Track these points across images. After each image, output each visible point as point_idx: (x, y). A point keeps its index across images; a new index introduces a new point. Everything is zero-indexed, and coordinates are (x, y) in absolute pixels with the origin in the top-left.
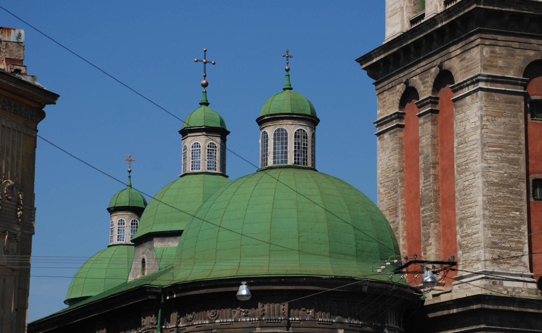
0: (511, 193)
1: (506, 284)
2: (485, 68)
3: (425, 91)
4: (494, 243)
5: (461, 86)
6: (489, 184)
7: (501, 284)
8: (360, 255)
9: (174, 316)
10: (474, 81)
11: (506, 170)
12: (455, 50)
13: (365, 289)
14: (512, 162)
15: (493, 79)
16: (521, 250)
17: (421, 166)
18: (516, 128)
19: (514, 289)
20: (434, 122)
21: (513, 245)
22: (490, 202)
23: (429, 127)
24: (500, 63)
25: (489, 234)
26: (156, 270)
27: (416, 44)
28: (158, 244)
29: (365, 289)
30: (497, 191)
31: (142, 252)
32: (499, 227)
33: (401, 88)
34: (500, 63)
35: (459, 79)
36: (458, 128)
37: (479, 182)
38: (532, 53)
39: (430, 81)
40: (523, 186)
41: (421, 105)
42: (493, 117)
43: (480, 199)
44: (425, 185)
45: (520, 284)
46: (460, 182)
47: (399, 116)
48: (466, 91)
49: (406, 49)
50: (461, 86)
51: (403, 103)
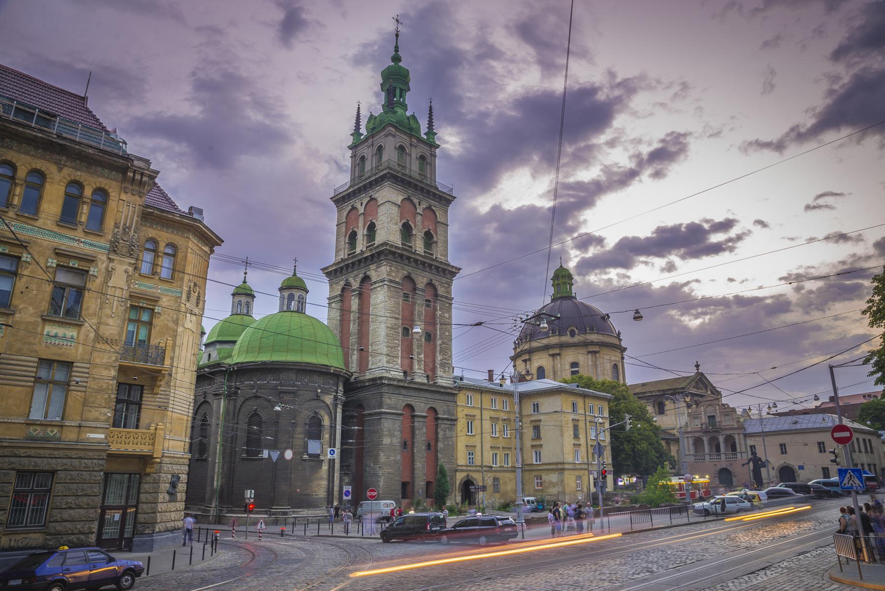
2: (388, 275)
3: (355, 284)
5: (375, 283)
6: (388, 327)
9: (234, 379)
10: (383, 281)
11: (393, 321)
12: (373, 267)
14: (396, 318)
15: (391, 281)
17: (352, 318)
18: (398, 304)
20: (360, 299)
22: (387, 335)
23: (357, 300)
25: (386, 349)
26: (218, 359)
27: (353, 264)
28: (218, 346)
31: (210, 349)
33: (342, 283)
35: (374, 280)
36: (372, 301)
37: (383, 326)
39: (359, 280)
40: (400, 330)
41: (354, 291)
42: (390, 297)
43: (383, 333)
44: (353, 327)
46: (372, 327)
47: (341, 295)
48: (378, 285)
49: (347, 266)
50: (375, 283)
51: (343, 290)
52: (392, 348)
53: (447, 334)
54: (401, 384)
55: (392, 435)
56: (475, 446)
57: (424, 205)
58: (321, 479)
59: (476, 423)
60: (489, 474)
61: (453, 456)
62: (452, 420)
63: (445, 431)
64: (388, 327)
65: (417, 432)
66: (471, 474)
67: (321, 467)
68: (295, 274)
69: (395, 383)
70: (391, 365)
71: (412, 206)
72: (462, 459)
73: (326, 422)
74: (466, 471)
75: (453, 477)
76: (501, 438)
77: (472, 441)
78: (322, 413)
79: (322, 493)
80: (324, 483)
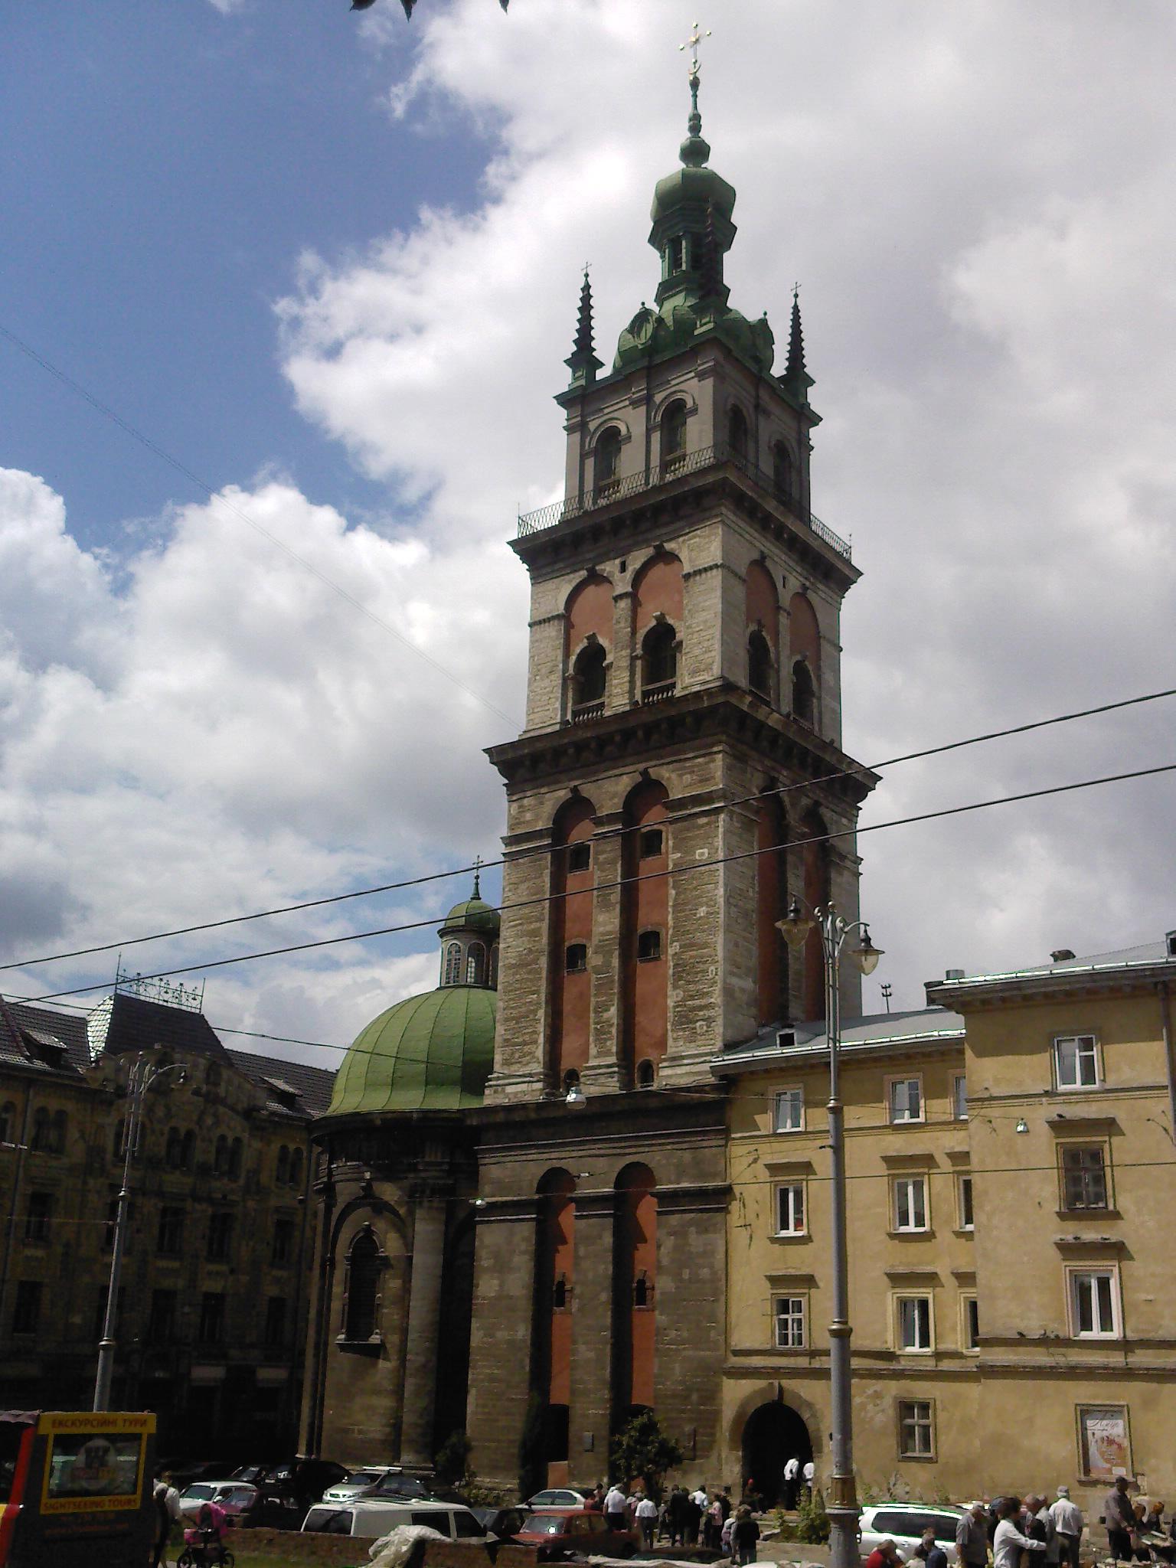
0: (529, 973)
1: (509, 1089)
4: (506, 1040)
7: (503, 1091)
8: (433, 1080)
13: (378, 1122)
14: (534, 933)
16: (535, 1042)
19: (516, 1094)
21: (527, 1038)
24: (528, 816)
29: (378, 1122)
30: (514, 974)
32: (513, 1019)
34: (528, 816)
38: (562, 793)
40: (544, 962)
45: (524, 1087)
52: (518, 1020)
53: (702, 911)
54: (517, 1117)
55: (502, 1267)
56: (809, 1281)
57: (637, 559)
58: (377, 1392)
59: (819, 1192)
60: (875, 1386)
61: (712, 1318)
62: (701, 1195)
63: (680, 1233)
64: (512, 966)
65: (582, 1251)
66: (786, 1383)
67: (375, 1365)
68: (477, 897)
69: (501, 1117)
70: (515, 1067)
71: (606, 585)
72: (750, 1324)
73: (391, 1245)
74: (776, 1372)
75: (711, 1395)
76: (945, 1237)
77: (797, 1261)
78: (380, 1226)
79: (375, 1428)
80: (385, 1403)
